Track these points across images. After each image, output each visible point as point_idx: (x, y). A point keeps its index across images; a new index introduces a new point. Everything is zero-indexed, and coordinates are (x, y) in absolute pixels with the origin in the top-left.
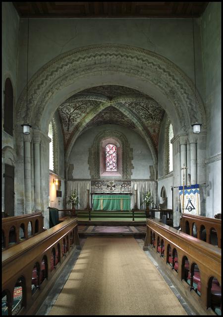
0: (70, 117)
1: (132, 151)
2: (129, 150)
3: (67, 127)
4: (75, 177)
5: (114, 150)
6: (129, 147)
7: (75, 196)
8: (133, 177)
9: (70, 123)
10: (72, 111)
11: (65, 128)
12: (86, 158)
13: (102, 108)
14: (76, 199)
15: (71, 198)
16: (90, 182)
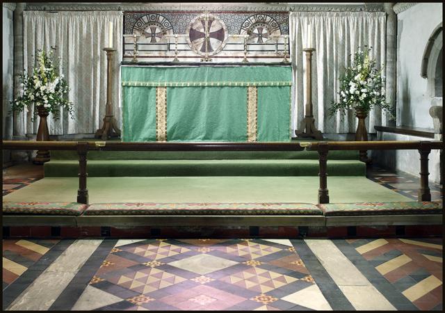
7: (49, 77)
14: (51, 87)
15: (31, 84)
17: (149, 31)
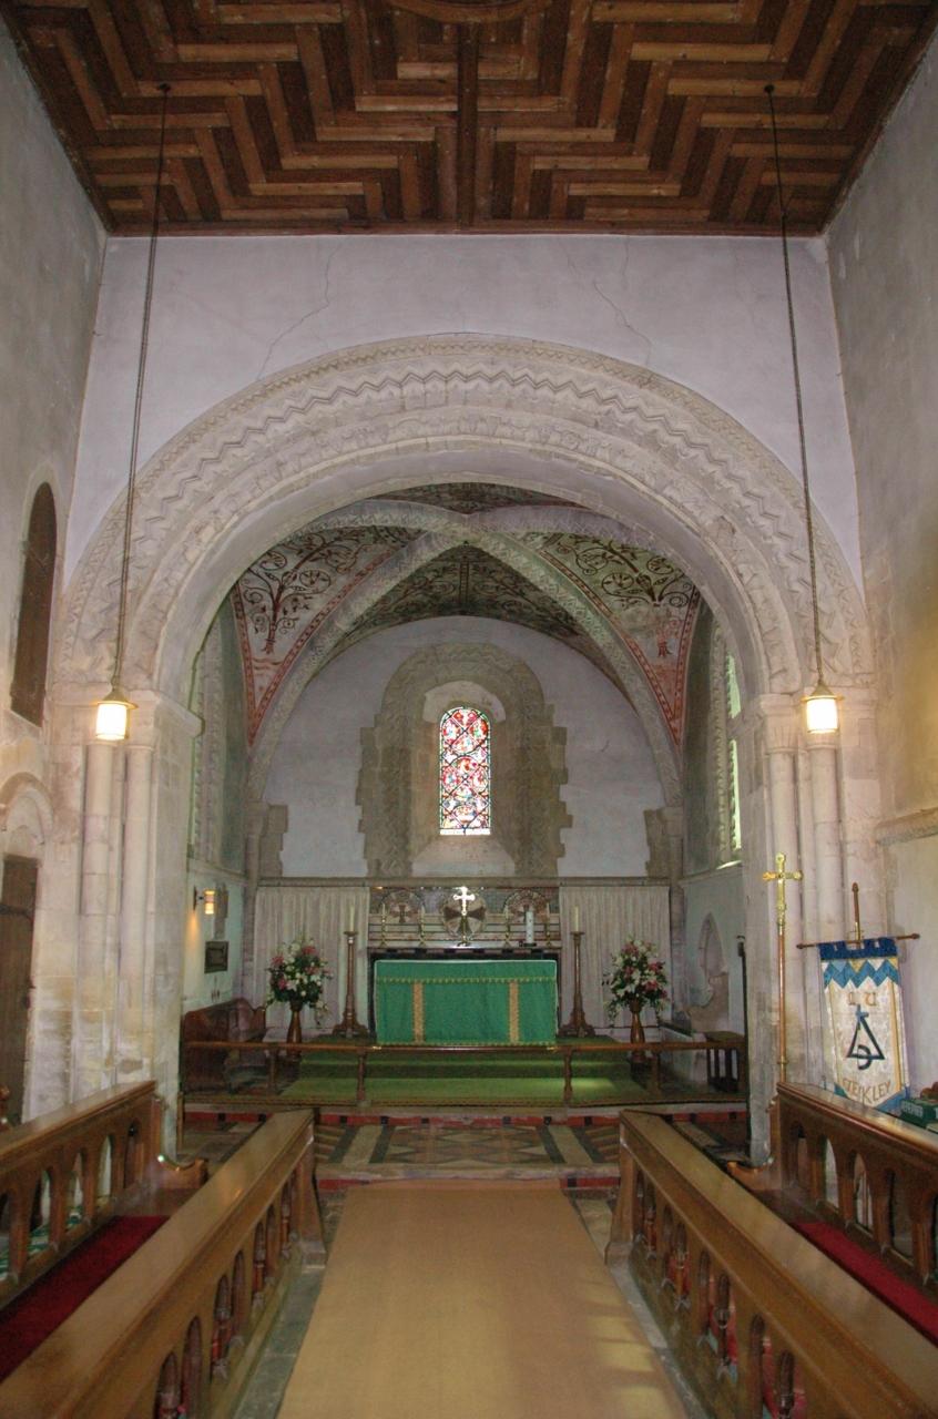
0: (282, 588)
1: (564, 743)
2: (549, 737)
3: (265, 635)
4: (292, 869)
5: (480, 733)
6: (549, 720)
8: (566, 868)
9: (280, 615)
10: (290, 567)
11: (257, 640)
12: (346, 775)
13: (425, 554)
16: (365, 896)
17: (397, 909)
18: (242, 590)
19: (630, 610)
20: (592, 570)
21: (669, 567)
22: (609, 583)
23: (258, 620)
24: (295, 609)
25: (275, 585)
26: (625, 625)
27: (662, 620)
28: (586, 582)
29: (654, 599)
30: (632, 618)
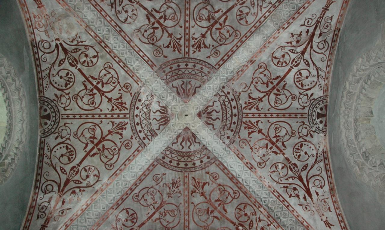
0: (303, 53)
3: (328, 14)
9: (311, 30)
10: (295, 70)
18: (327, 53)
19: (73, 34)
20: (108, 67)
21: (61, 77)
22: (94, 57)
23: (327, 26)
24: (301, 34)
25: (307, 56)
26: (73, 20)
27: (49, 27)
28: (108, 56)
29: (61, 44)
30: (70, 26)
